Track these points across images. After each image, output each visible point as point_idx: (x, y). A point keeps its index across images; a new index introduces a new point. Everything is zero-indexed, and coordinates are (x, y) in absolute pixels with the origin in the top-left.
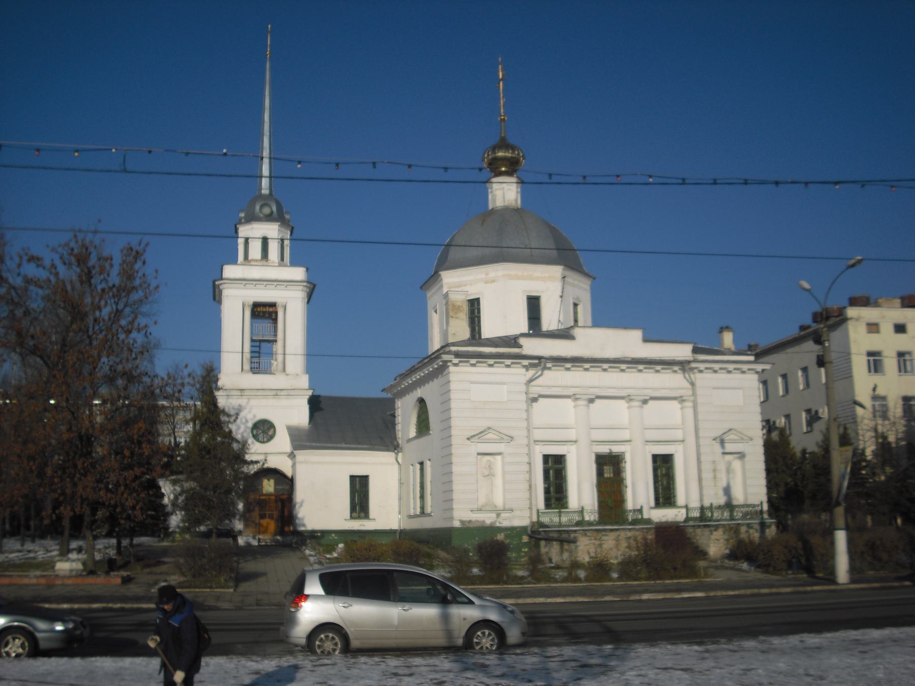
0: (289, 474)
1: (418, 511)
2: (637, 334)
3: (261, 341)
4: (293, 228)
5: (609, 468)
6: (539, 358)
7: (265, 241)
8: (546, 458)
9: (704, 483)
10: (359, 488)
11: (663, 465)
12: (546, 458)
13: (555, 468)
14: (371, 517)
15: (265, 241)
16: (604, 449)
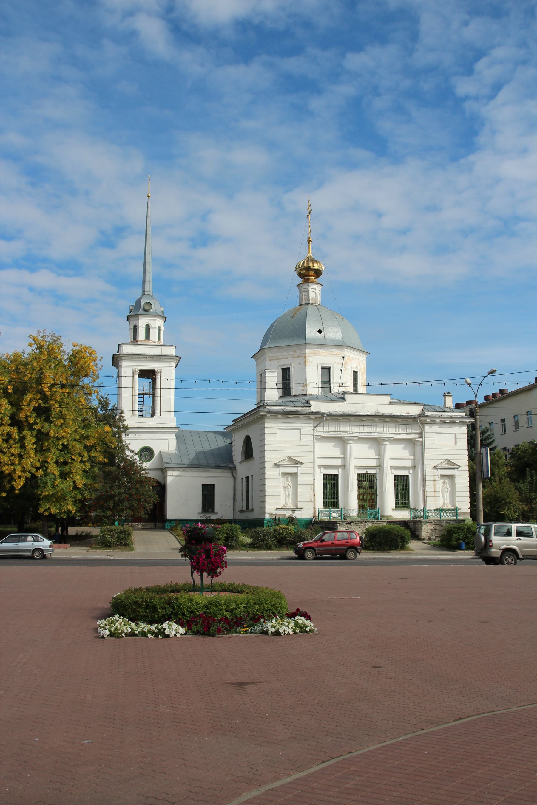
0: (162, 483)
1: (245, 508)
2: (387, 399)
3: (144, 394)
4: (166, 318)
5: (368, 483)
6: (323, 414)
7: (148, 328)
8: (326, 476)
9: (428, 494)
10: (208, 492)
11: (402, 483)
12: (326, 476)
13: (331, 483)
14: (215, 511)
15: (148, 328)
16: (363, 471)
